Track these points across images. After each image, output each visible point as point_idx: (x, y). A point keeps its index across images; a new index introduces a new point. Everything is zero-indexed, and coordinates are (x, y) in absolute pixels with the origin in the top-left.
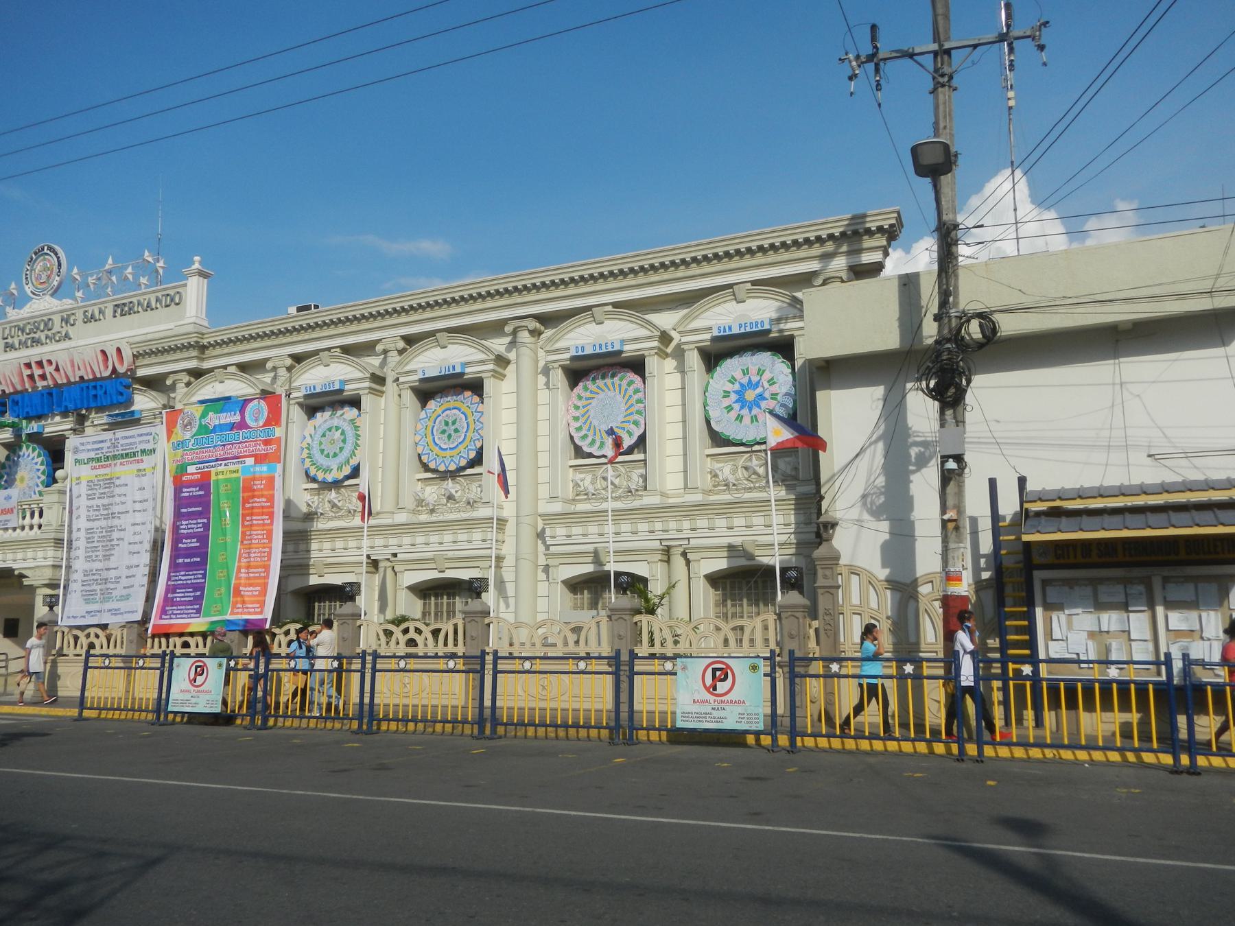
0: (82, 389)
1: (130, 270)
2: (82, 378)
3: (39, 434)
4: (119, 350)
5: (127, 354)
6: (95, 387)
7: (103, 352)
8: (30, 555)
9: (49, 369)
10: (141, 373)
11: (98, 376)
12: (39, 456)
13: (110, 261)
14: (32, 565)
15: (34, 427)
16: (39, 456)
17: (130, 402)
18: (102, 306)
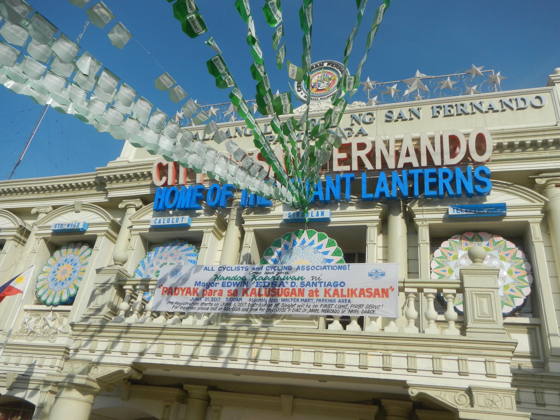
0: (411, 178)
1: (449, 79)
2: (408, 166)
3: (327, 220)
4: (481, 139)
5: (490, 143)
6: (432, 175)
7: (454, 141)
8: (449, 364)
9: (355, 153)
10: (493, 168)
11: (437, 162)
12: (329, 245)
13: (418, 72)
14: (465, 383)
15: (313, 213)
16: (329, 245)
17: (482, 196)
18: (415, 108)
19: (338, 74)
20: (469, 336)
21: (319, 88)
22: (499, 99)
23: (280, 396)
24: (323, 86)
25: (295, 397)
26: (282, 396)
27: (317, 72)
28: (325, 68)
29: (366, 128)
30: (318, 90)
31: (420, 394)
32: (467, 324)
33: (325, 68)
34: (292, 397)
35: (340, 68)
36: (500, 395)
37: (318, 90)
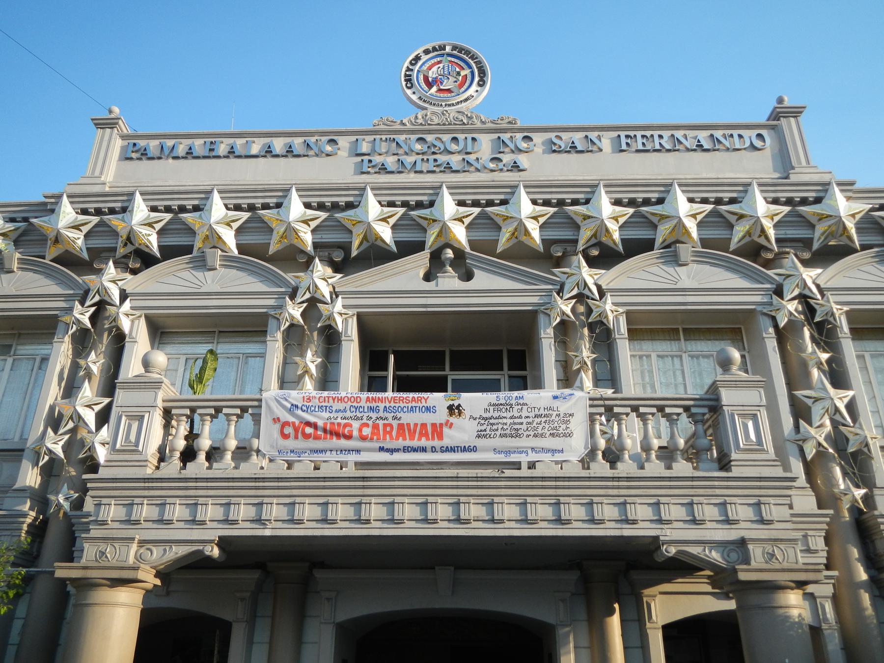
19: (470, 67)
20: (735, 472)
21: (442, 87)
22: (709, 132)
23: (434, 568)
24: (448, 84)
25: (457, 568)
26: (437, 568)
27: (435, 60)
28: (449, 55)
29: (523, 160)
30: (440, 90)
31: (679, 552)
32: (729, 456)
33: (449, 55)
34: (452, 568)
35: (472, 58)
36: (781, 546)
37: (440, 90)
